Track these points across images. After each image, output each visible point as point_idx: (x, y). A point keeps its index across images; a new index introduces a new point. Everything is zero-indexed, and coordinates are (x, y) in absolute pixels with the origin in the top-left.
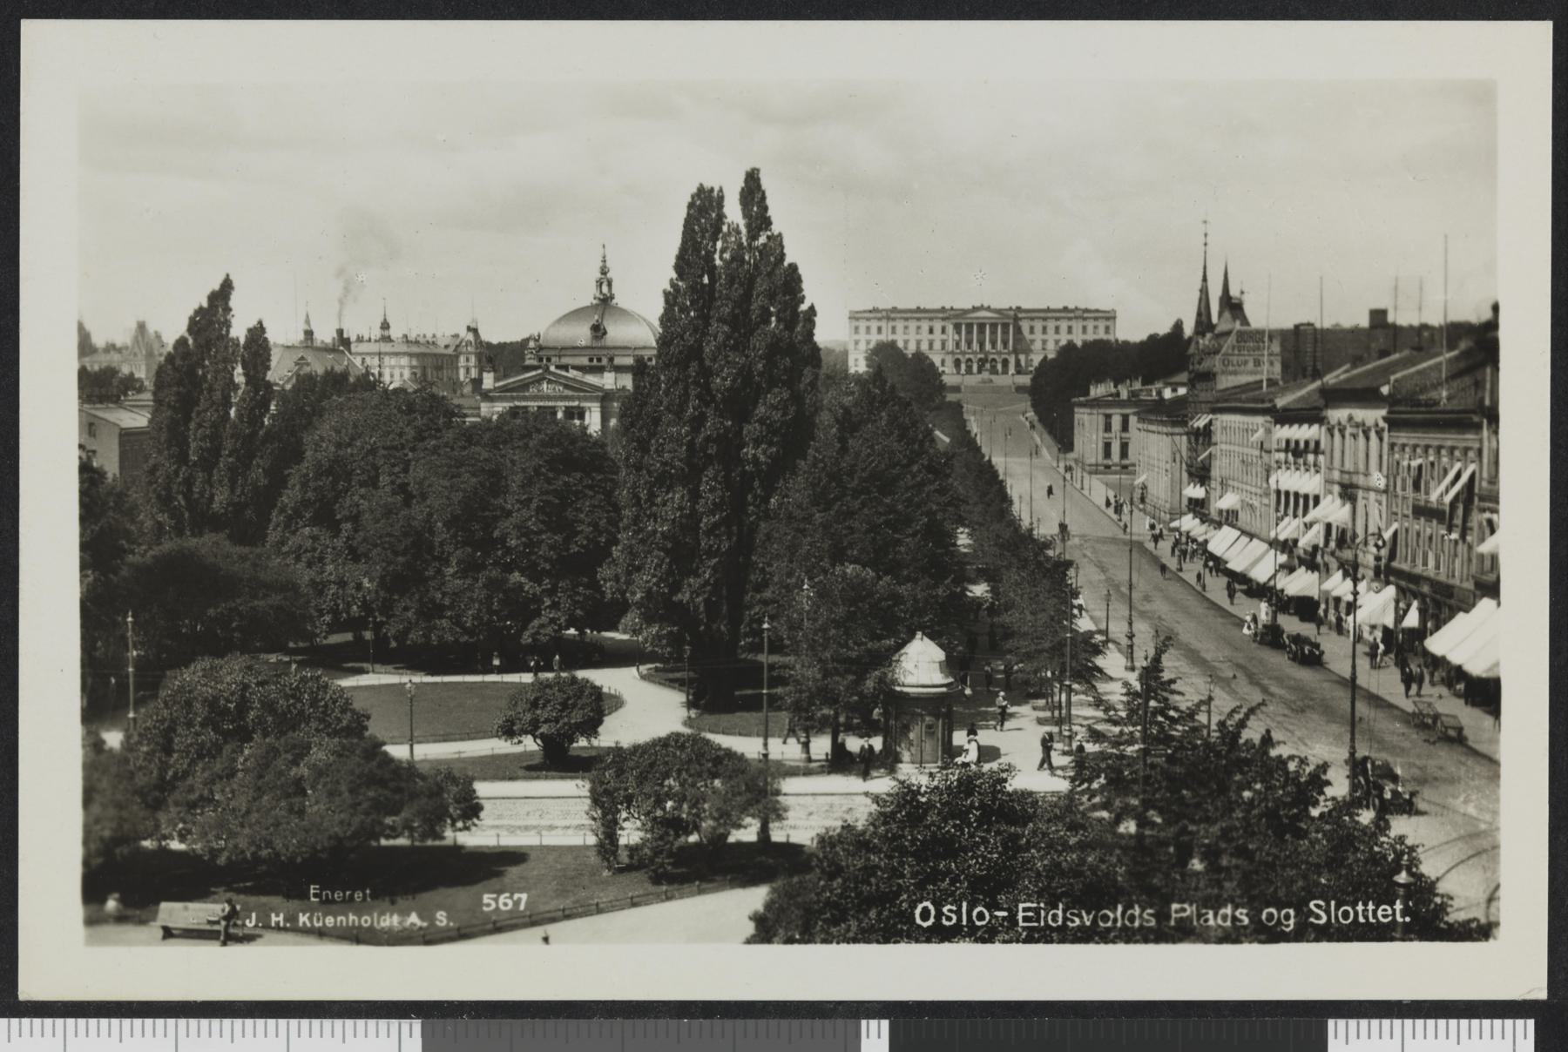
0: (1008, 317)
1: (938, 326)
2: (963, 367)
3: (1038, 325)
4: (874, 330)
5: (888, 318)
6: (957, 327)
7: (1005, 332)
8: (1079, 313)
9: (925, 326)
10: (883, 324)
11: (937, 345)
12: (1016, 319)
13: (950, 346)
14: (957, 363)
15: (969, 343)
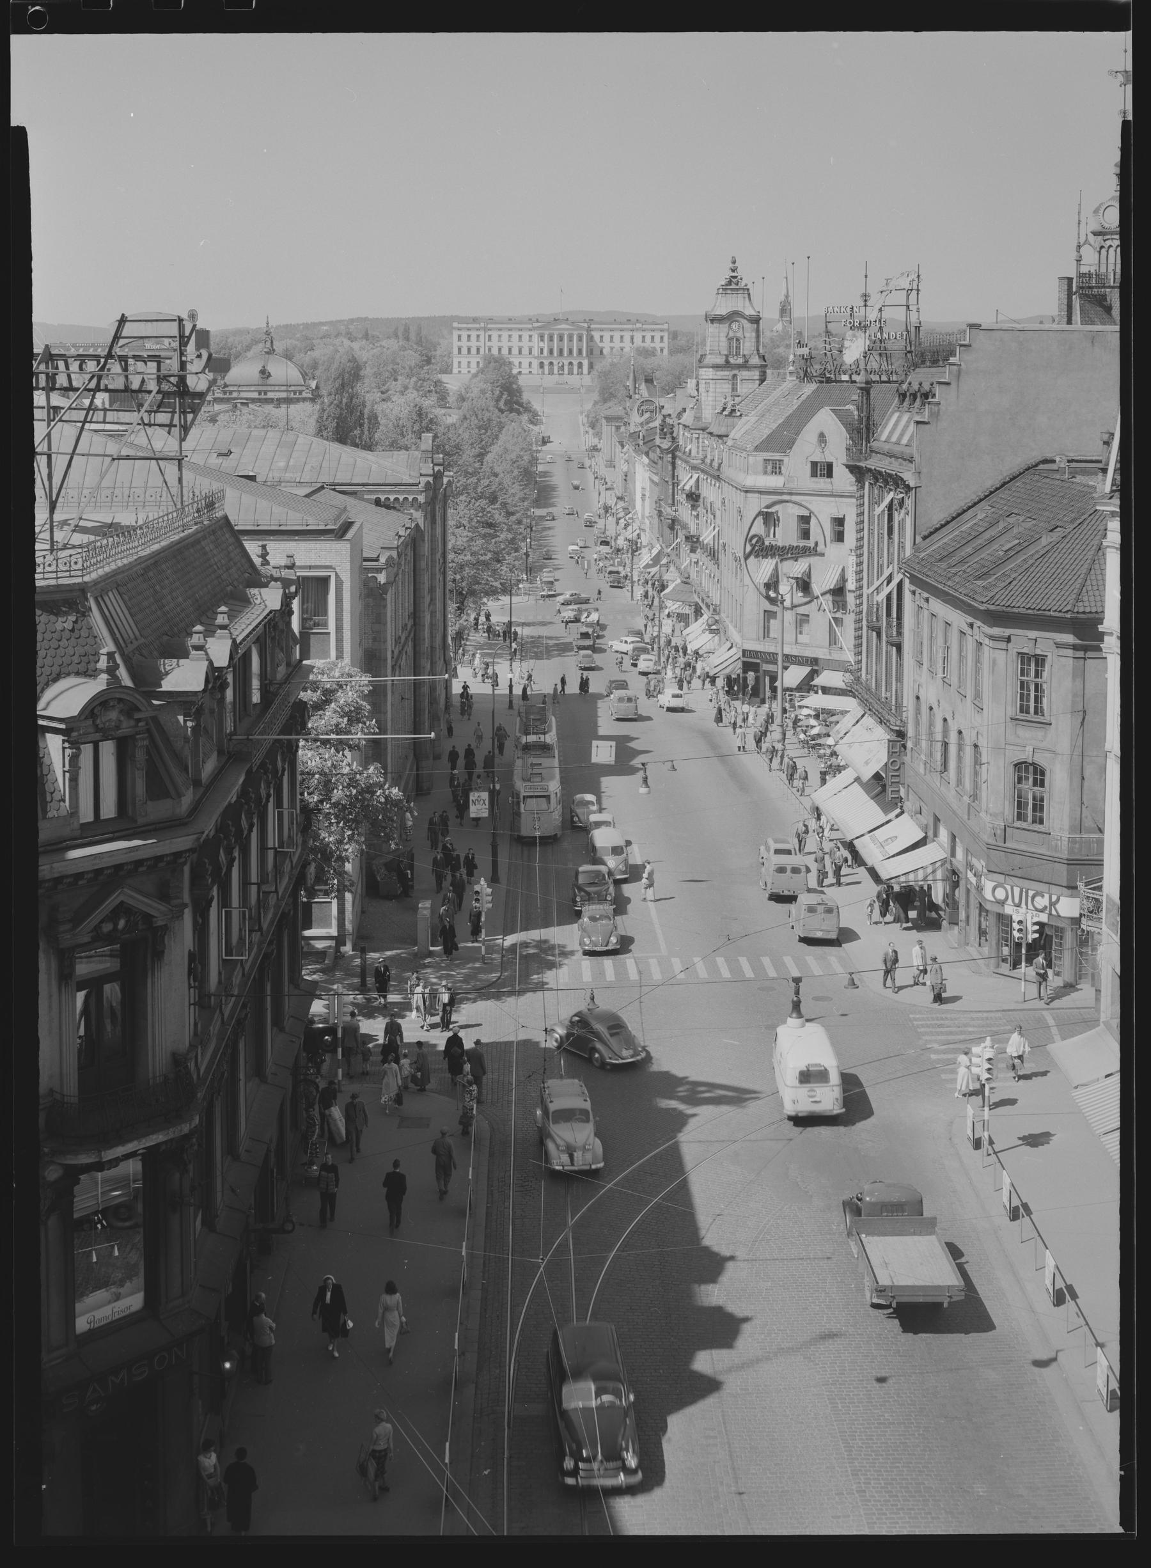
0: (582, 328)
1: (526, 335)
2: (546, 368)
3: (607, 336)
4: (473, 338)
5: (485, 329)
6: (542, 338)
7: (580, 339)
8: (639, 325)
9: (515, 335)
10: (482, 333)
11: (525, 351)
12: (589, 329)
13: (536, 352)
14: (542, 365)
15: (551, 352)
